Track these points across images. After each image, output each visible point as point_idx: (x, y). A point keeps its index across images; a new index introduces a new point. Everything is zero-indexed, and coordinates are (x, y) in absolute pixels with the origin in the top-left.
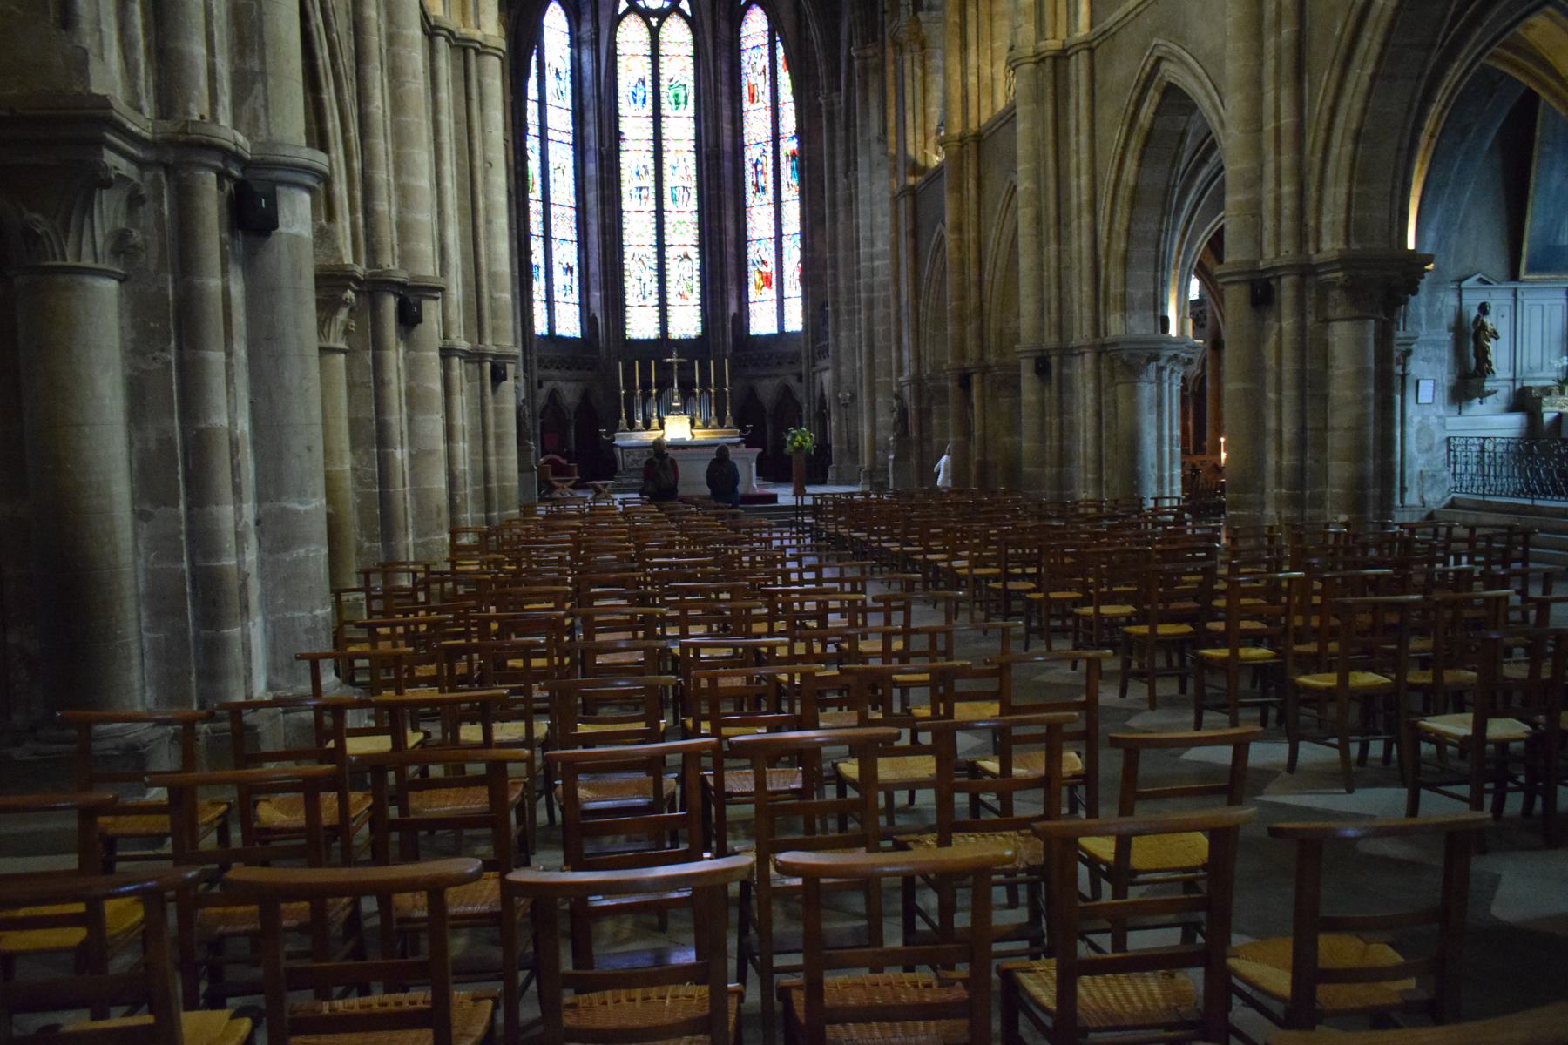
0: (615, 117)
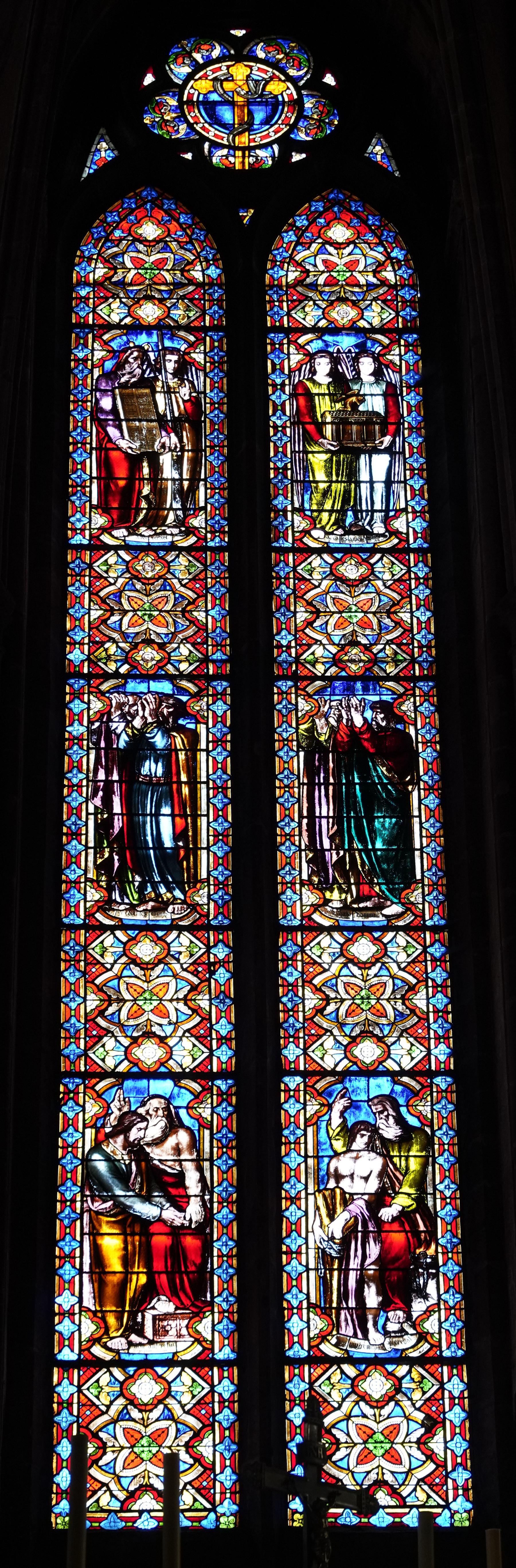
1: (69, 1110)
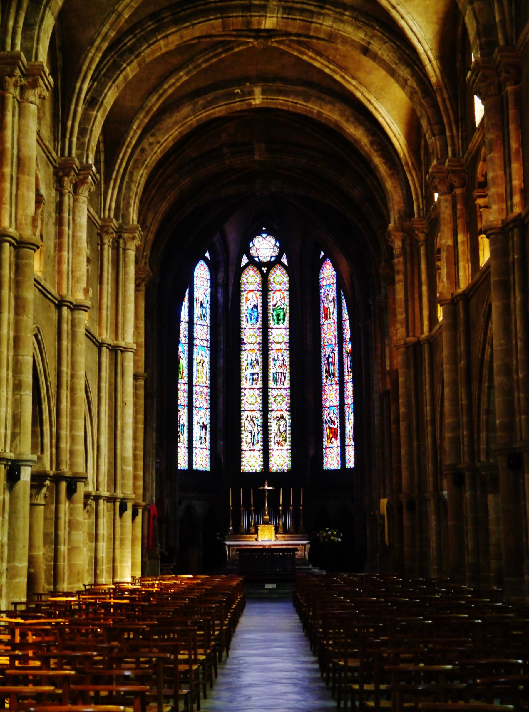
0: (237, 329)
1: (324, 413)
